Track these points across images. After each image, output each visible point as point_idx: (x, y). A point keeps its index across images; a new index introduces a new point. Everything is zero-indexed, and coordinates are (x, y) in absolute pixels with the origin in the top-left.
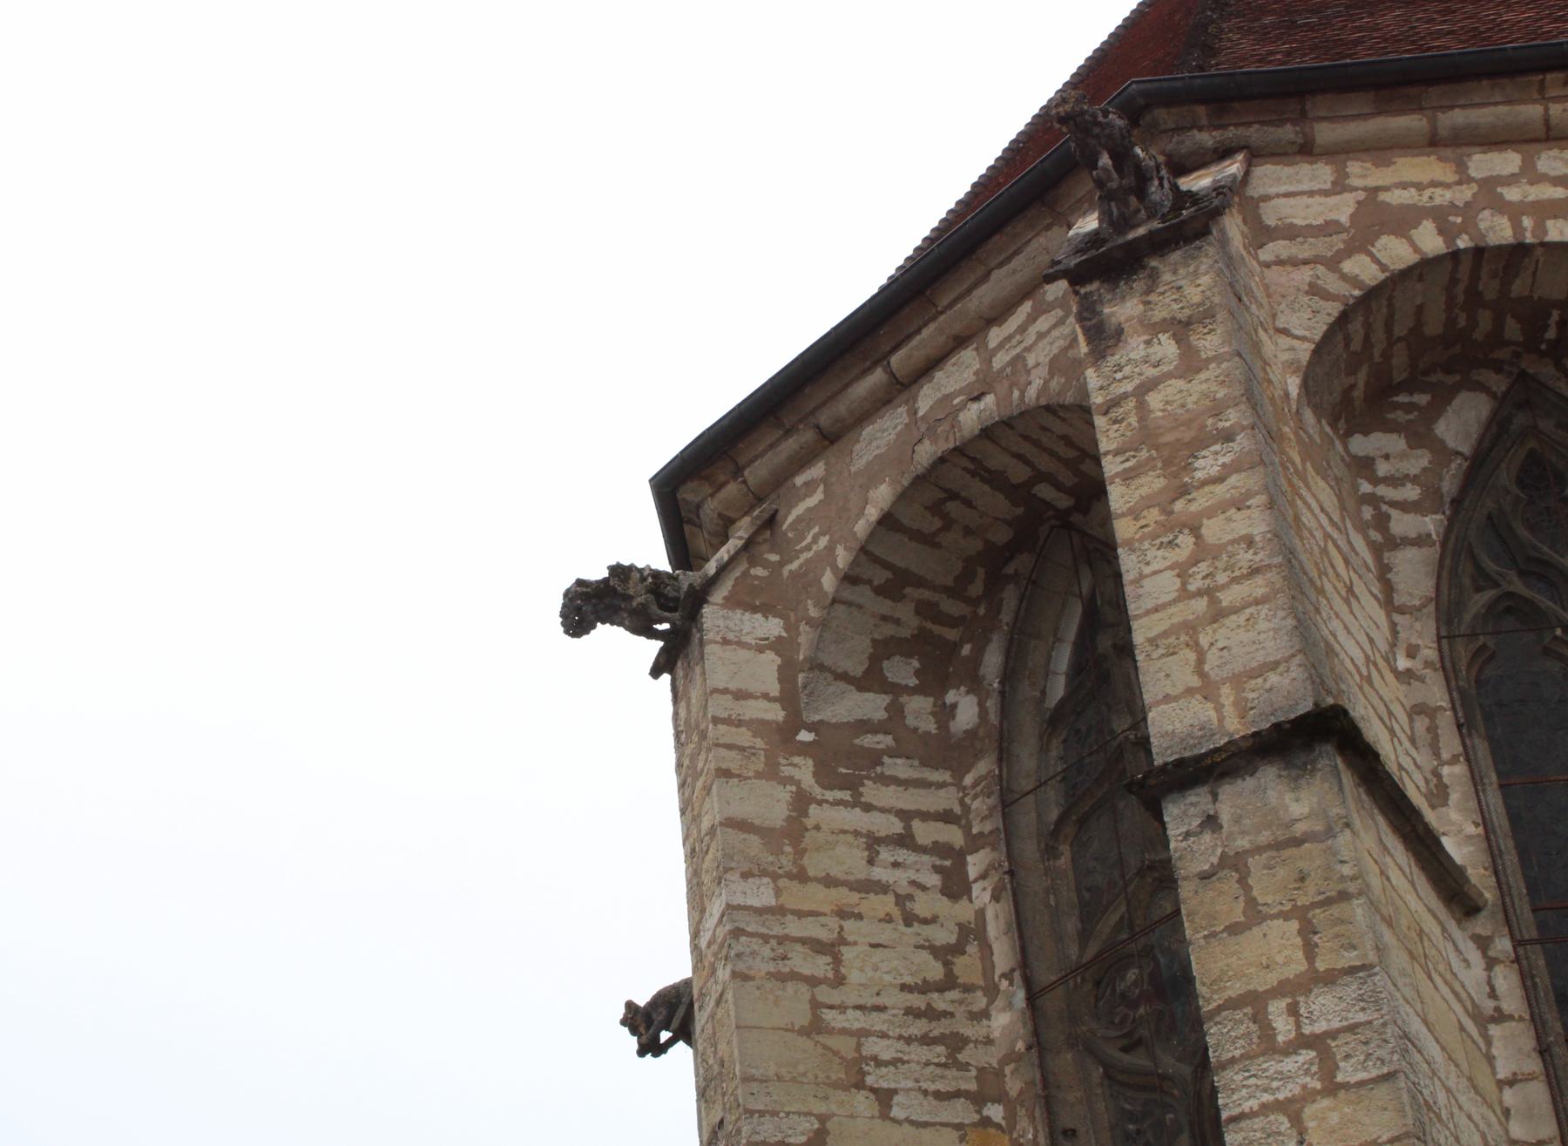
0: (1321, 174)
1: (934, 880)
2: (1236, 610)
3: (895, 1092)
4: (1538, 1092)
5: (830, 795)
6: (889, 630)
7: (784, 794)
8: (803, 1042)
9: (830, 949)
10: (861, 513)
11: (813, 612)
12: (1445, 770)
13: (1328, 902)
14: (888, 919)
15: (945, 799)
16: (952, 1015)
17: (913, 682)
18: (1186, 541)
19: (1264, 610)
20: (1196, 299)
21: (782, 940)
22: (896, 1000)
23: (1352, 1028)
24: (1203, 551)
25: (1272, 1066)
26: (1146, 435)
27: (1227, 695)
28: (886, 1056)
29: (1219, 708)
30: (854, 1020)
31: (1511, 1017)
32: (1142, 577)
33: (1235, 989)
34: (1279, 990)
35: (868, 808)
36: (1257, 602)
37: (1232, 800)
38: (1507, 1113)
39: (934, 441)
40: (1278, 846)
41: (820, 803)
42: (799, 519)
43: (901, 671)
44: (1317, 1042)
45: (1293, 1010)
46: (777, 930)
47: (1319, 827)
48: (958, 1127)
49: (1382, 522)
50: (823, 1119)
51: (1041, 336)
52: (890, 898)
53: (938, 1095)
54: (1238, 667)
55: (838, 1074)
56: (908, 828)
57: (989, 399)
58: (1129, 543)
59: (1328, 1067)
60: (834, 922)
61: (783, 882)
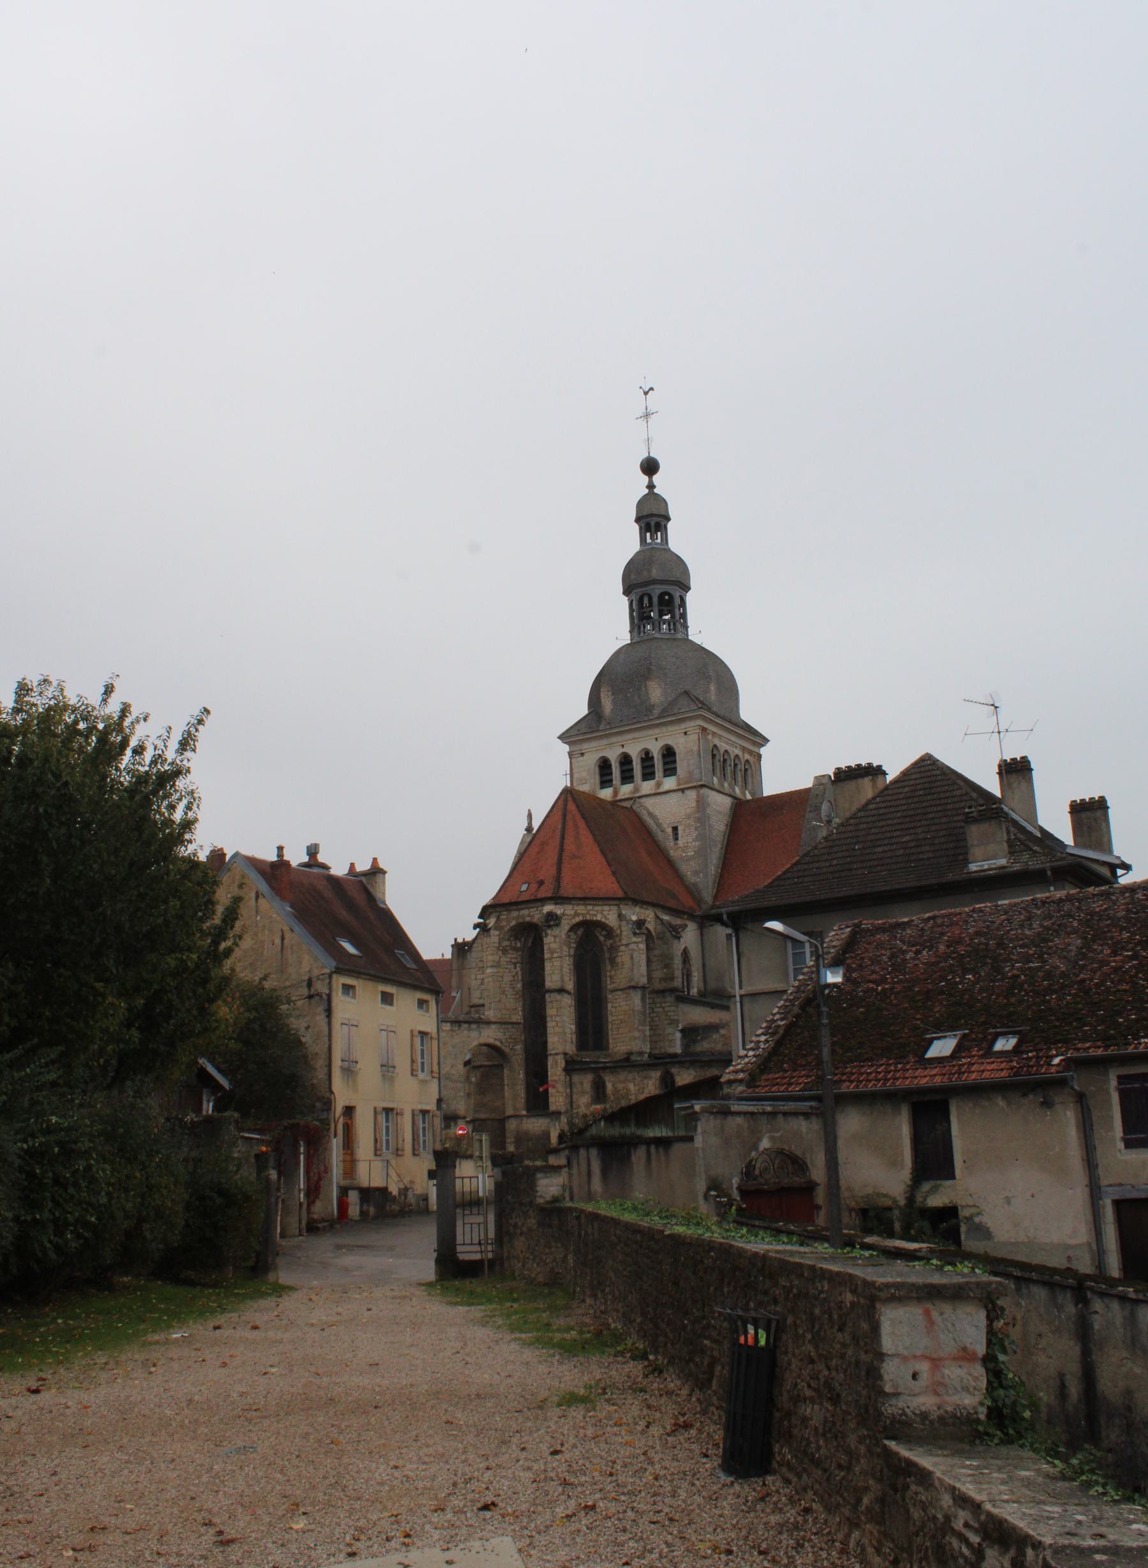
0: (570, 907)
9: (502, 977)
15: (514, 956)
37: (553, 995)
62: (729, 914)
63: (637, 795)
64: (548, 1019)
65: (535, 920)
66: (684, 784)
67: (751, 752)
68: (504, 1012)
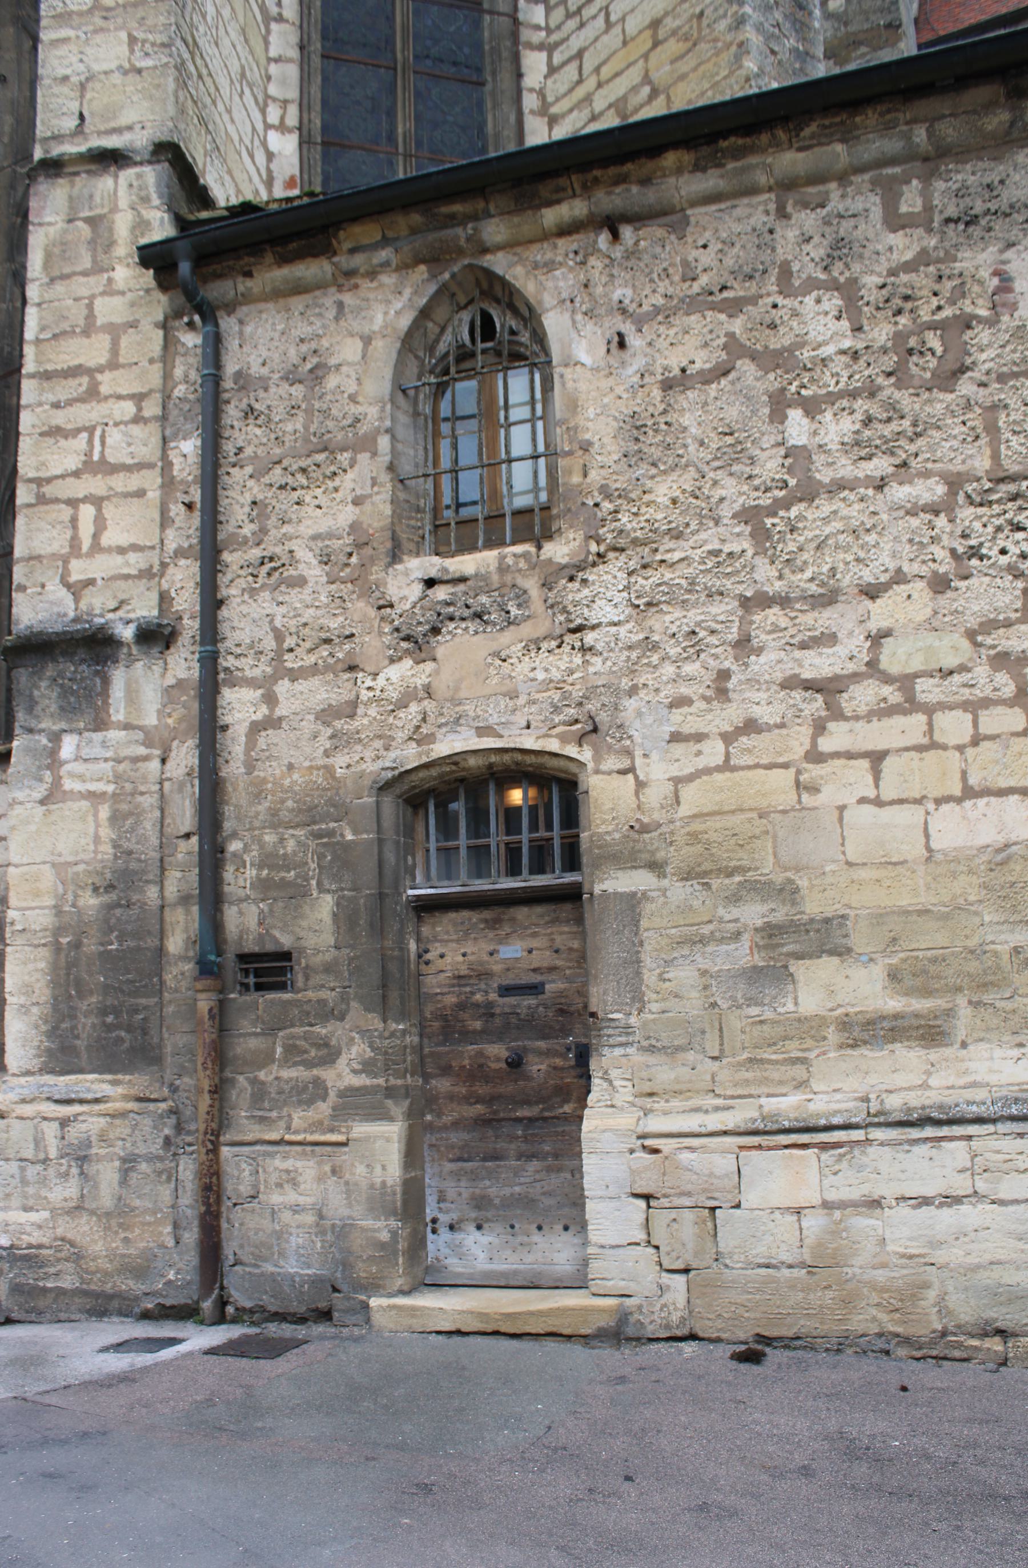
4: (292, 71)
31: (287, 21)
38: (269, 78)
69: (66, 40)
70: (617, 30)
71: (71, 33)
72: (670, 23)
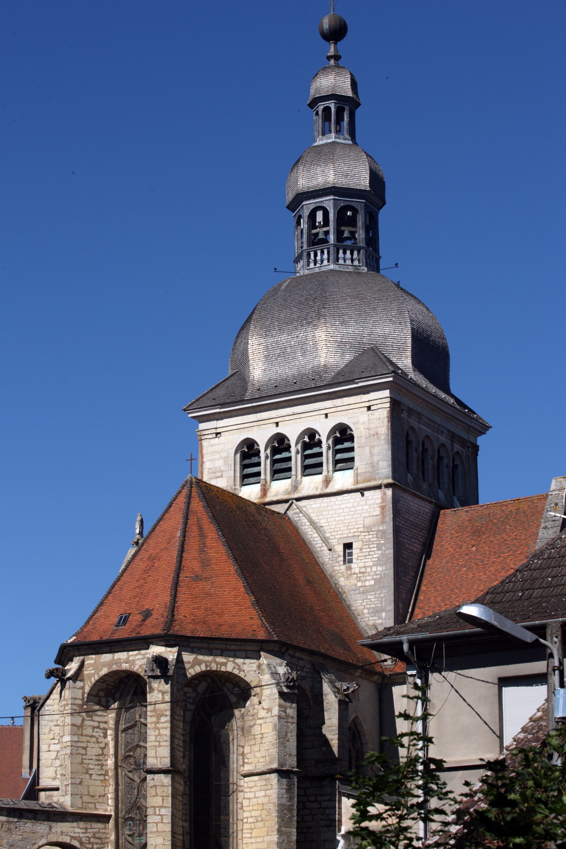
1: (102, 735)
2: (162, 746)
3: (92, 774)
5: (88, 719)
6: (101, 687)
7: (81, 719)
8: (80, 766)
9: (85, 748)
10: (101, 671)
11: (89, 684)
12: (186, 753)
13: (166, 796)
14: (94, 743)
16: (102, 760)
17: (103, 695)
18: (157, 731)
19: (166, 748)
20: (166, 688)
21: (78, 747)
22: (94, 757)
23: (166, 815)
24: (159, 734)
25: (155, 817)
26: (154, 710)
27: (159, 759)
28: (92, 768)
29: (157, 761)
30: (87, 761)
32: (150, 735)
33: (152, 805)
34: (158, 807)
35: (93, 721)
36: (165, 746)
37: (157, 776)
39: (117, 665)
40: (162, 786)
41: (86, 720)
42: (88, 664)
43: (102, 694)
44: (162, 816)
45: (159, 810)
46: (77, 745)
47: (167, 785)
48: (101, 780)
49: (186, 705)
50: (82, 779)
51: (139, 659)
52: (95, 739)
53: (99, 775)
54: (161, 756)
55: (84, 771)
56: (99, 725)
57: (127, 665)
58: (149, 728)
59: (162, 819)
60: (86, 743)
61: (79, 736)
62: (412, 643)
63: (296, 496)
64: (150, 811)
65: (136, 668)
66: (364, 481)
67: (463, 442)
68: (86, 799)
69: (152, 837)
70: (256, 799)
71: (153, 836)
72: (265, 807)
